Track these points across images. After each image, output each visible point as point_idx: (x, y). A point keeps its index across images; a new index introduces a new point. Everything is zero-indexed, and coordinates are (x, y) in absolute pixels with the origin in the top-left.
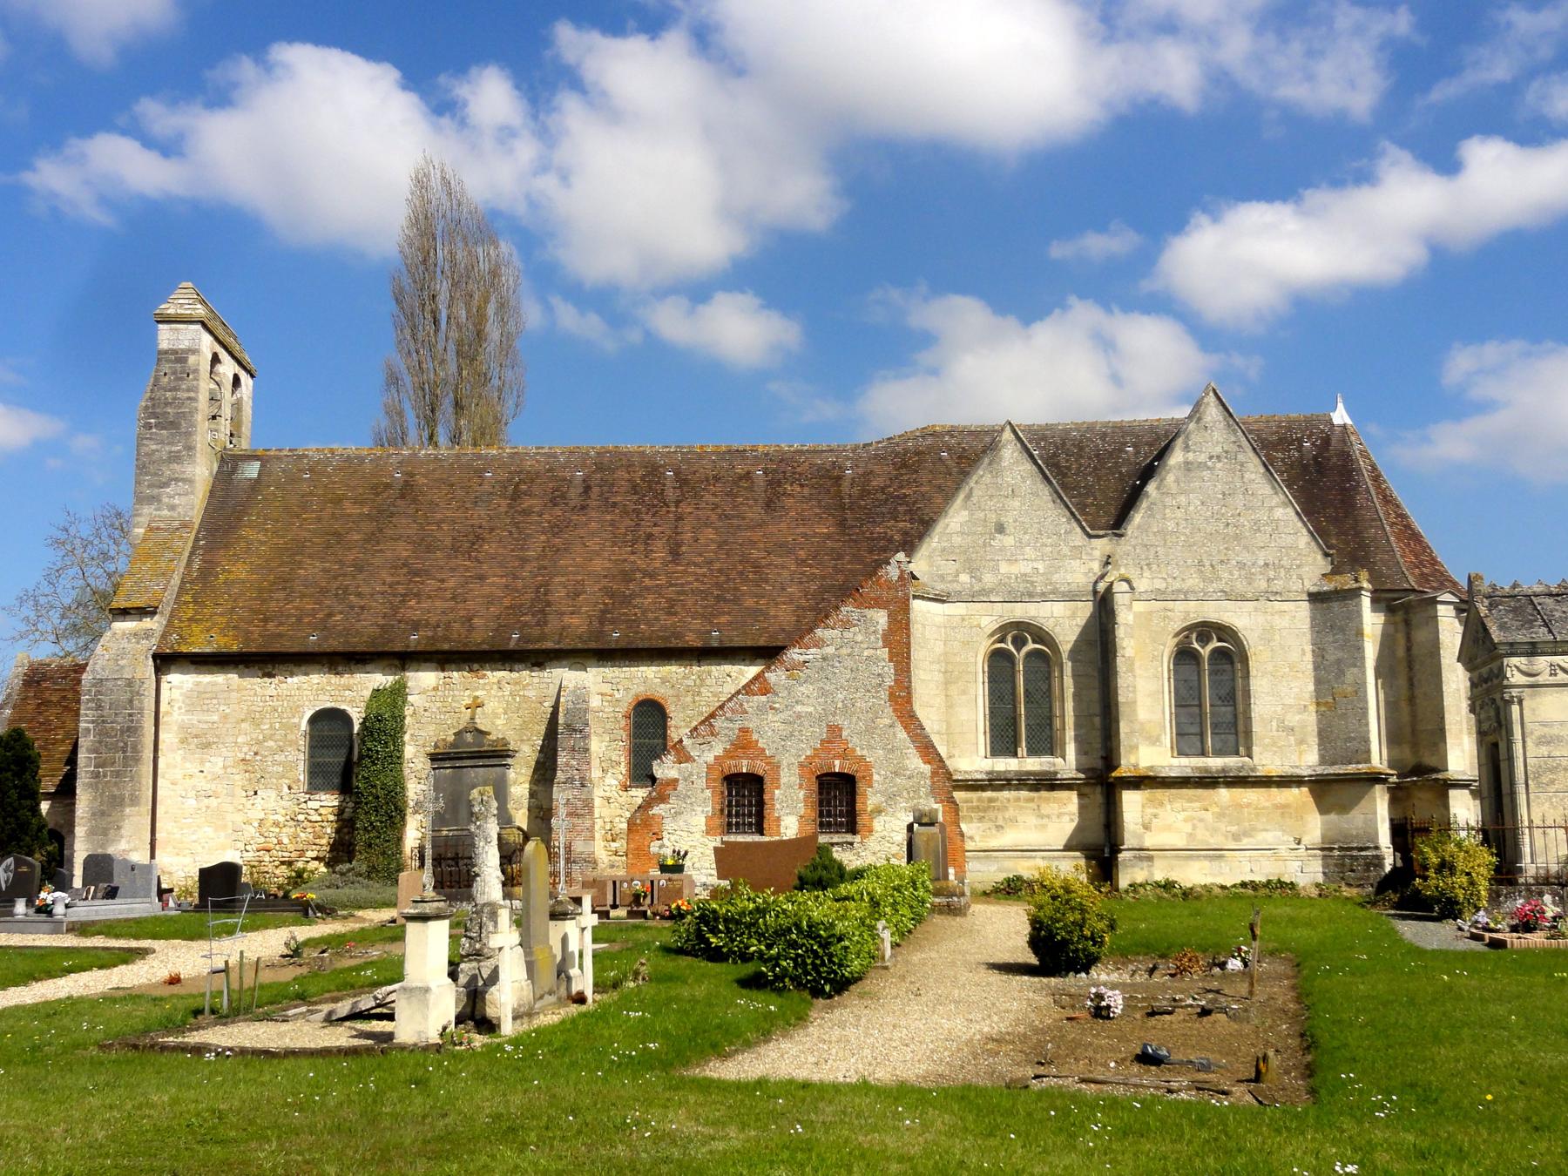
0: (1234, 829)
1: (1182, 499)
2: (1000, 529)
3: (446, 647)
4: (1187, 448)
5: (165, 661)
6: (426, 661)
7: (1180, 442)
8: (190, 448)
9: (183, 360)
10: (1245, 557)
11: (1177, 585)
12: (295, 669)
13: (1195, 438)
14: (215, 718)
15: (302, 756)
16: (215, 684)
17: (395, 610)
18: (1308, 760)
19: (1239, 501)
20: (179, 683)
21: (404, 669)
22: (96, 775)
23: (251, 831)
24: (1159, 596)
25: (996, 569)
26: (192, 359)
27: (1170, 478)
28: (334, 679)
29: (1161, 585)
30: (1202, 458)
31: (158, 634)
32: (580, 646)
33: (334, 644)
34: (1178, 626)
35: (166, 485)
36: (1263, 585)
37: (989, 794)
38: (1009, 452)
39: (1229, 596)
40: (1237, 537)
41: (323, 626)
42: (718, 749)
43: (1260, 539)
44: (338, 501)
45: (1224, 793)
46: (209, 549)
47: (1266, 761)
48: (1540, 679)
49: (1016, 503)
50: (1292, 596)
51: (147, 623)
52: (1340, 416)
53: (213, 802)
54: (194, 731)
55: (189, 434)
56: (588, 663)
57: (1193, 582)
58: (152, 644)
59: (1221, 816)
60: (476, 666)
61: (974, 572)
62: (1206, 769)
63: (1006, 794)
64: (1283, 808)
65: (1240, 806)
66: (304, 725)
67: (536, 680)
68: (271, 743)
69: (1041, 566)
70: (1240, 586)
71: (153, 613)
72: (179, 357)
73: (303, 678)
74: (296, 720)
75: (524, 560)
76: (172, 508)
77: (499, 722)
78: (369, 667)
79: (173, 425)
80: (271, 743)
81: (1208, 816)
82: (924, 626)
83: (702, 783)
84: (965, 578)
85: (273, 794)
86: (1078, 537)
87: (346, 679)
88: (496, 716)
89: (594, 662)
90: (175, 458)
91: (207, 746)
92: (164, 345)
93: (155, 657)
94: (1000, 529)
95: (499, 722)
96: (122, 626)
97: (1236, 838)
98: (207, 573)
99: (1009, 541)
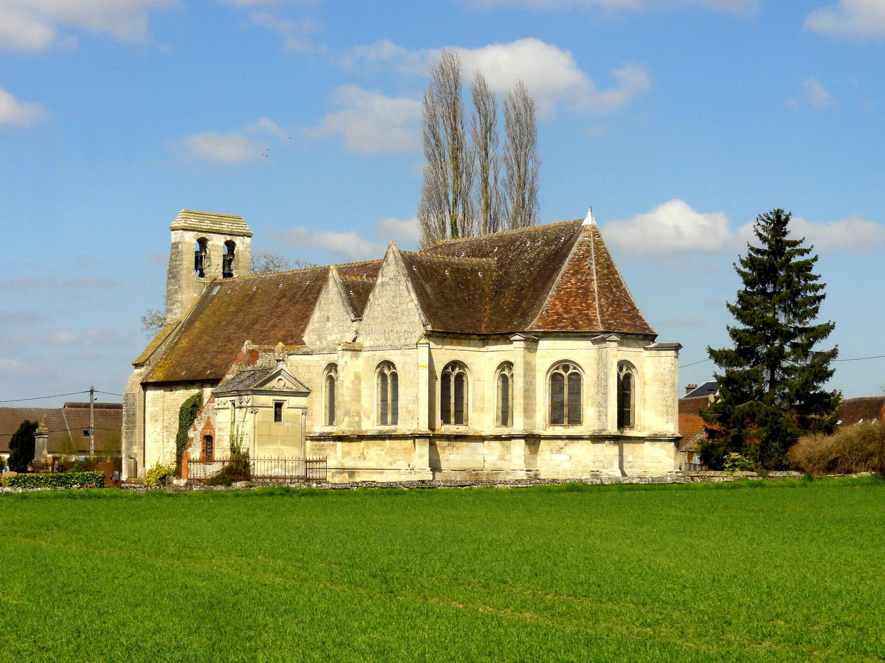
0: (390, 459)
1: (380, 300)
2: (328, 320)
3: (211, 377)
4: (383, 276)
5: (145, 386)
7: (380, 272)
8: (180, 287)
9: (177, 247)
10: (399, 328)
11: (377, 343)
13: (385, 270)
17: (213, 358)
18: (423, 427)
19: (397, 300)
20: (150, 393)
21: (203, 387)
22: (127, 433)
23: (168, 456)
24: (373, 349)
25: (326, 338)
26: (180, 246)
27: (377, 291)
29: (372, 343)
30: (387, 280)
31: (144, 375)
33: (186, 378)
34: (377, 363)
35: (173, 304)
36: (403, 341)
37: (322, 443)
38: (331, 283)
39: (394, 348)
40: (397, 318)
41: (189, 369)
42: (202, 426)
43: (404, 318)
44: (229, 306)
45: (387, 441)
46: (184, 332)
47: (403, 428)
48: (220, 407)
49: (332, 307)
50: (412, 346)
51: (143, 370)
52: (588, 221)
53: (158, 444)
55: (179, 281)
57: (382, 342)
58: (139, 380)
59: (387, 453)
61: (320, 339)
62: (381, 431)
63: (327, 443)
64: (405, 449)
65: (393, 449)
69: (338, 336)
70: (397, 343)
71: (143, 366)
72: (175, 246)
75: (262, 332)
76: (176, 314)
79: (175, 277)
81: (383, 453)
82: (297, 367)
83: (199, 439)
84: (318, 343)
86: (349, 323)
90: (176, 292)
91: (156, 421)
92: (173, 241)
93: (142, 384)
94: (328, 320)
96: (138, 371)
97: (391, 464)
98: (176, 344)
99: (329, 324)
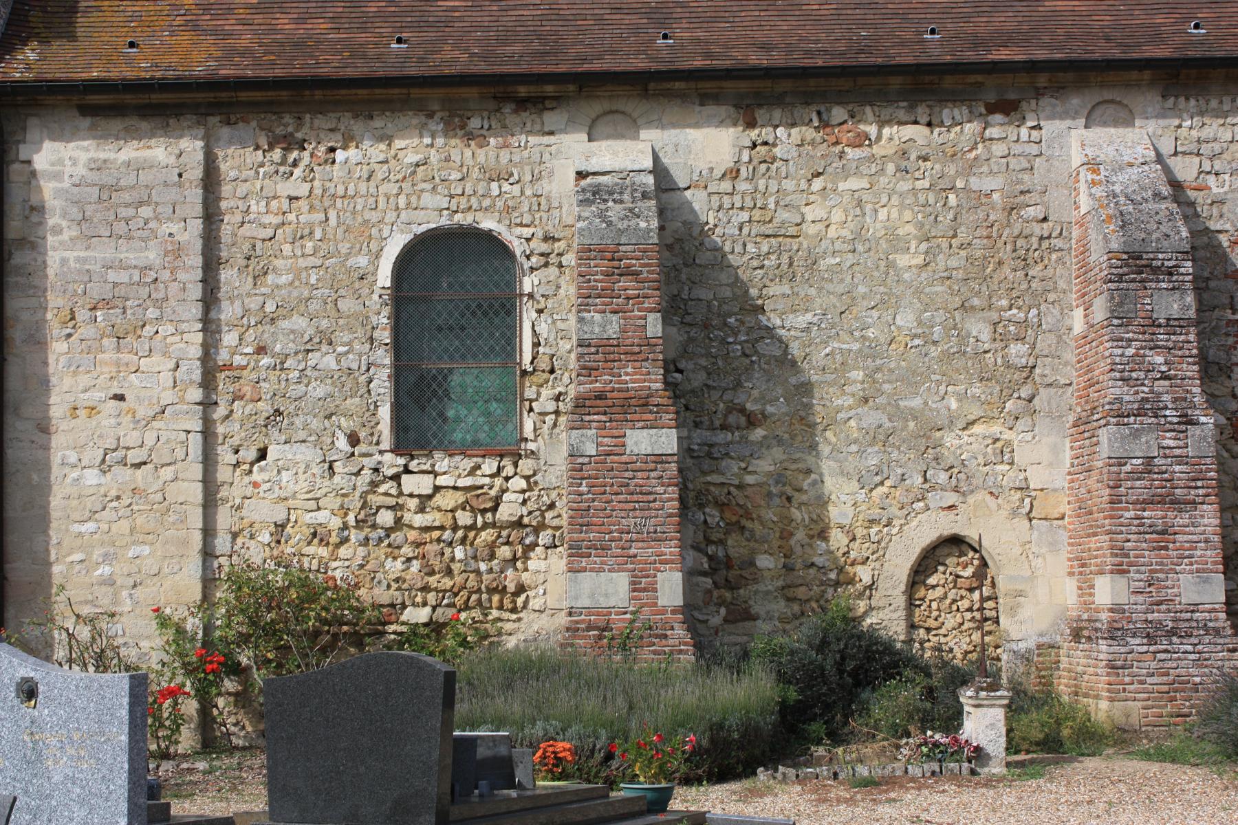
6: (705, 99)
12: (357, 126)
14: (152, 255)
15: (384, 358)
16: (148, 166)
28: (459, 150)
32: (1116, 53)
54: (96, 291)
56: (1137, 100)
60: (839, 113)
66: (384, 277)
67: (999, 149)
68: (298, 322)
73: (377, 151)
74: (362, 261)
77: (902, 260)
78: (551, 119)
80: (298, 322)
85: (307, 454)
87: (491, 152)
88: (897, 243)
89: (1152, 100)
95: (902, 260)
